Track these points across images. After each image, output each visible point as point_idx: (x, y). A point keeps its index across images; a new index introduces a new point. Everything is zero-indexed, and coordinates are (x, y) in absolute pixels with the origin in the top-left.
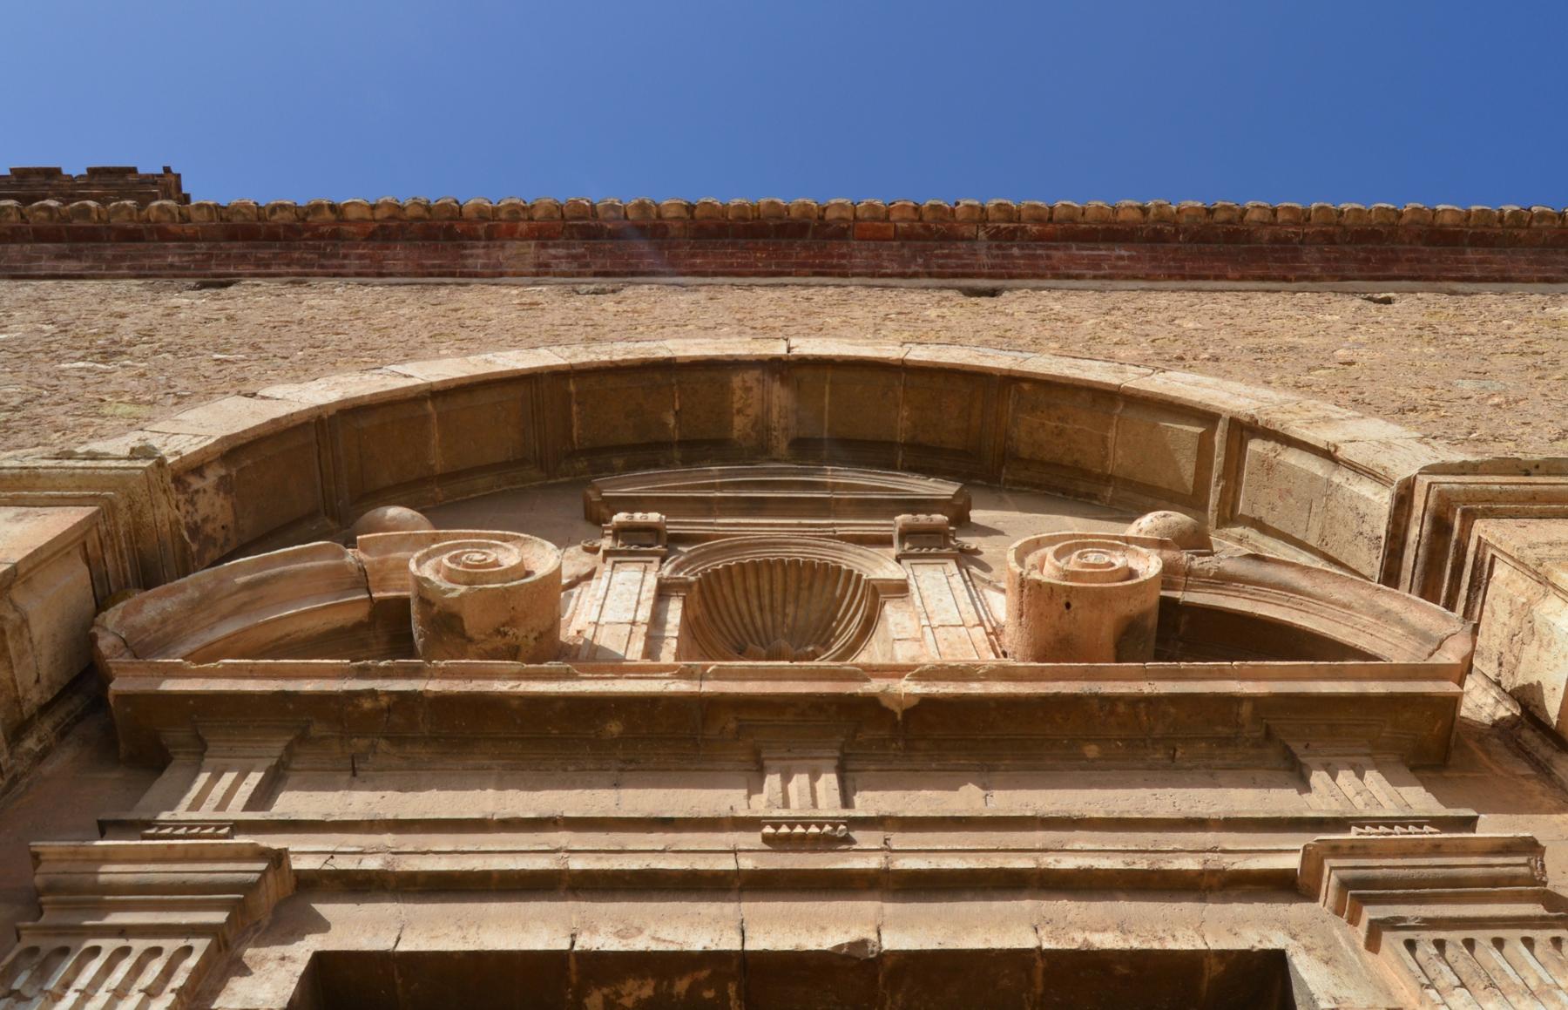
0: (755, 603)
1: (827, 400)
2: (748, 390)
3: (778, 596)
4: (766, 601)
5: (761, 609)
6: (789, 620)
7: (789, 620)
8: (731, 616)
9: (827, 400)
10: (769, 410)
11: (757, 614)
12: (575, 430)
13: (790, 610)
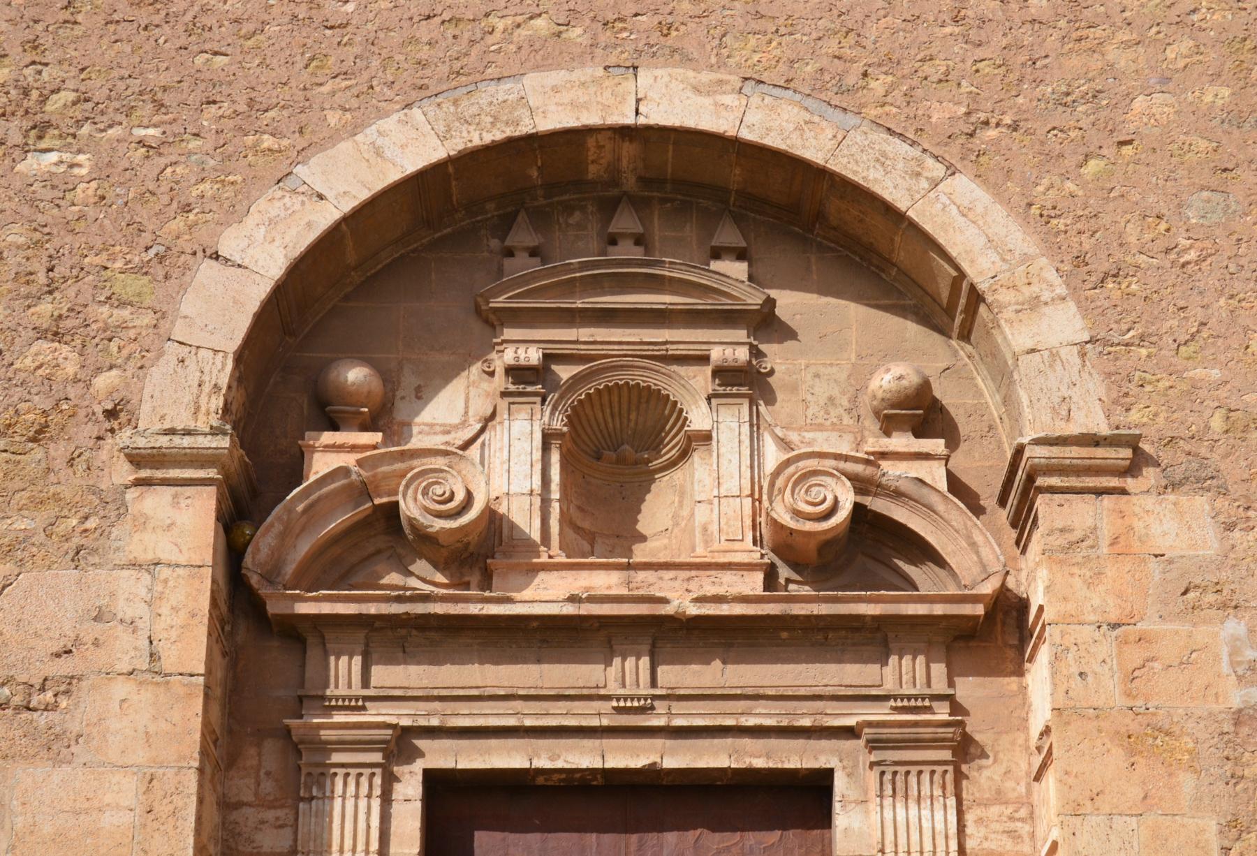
0: (608, 411)
1: (670, 154)
2: (600, 147)
3: (625, 407)
4: (616, 410)
5: (613, 416)
6: (632, 424)
7: (632, 424)
8: (591, 427)
9: (670, 154)
10: (619, 159)
11: (610, 420)
12: (454, 199)
13: (633, 416)
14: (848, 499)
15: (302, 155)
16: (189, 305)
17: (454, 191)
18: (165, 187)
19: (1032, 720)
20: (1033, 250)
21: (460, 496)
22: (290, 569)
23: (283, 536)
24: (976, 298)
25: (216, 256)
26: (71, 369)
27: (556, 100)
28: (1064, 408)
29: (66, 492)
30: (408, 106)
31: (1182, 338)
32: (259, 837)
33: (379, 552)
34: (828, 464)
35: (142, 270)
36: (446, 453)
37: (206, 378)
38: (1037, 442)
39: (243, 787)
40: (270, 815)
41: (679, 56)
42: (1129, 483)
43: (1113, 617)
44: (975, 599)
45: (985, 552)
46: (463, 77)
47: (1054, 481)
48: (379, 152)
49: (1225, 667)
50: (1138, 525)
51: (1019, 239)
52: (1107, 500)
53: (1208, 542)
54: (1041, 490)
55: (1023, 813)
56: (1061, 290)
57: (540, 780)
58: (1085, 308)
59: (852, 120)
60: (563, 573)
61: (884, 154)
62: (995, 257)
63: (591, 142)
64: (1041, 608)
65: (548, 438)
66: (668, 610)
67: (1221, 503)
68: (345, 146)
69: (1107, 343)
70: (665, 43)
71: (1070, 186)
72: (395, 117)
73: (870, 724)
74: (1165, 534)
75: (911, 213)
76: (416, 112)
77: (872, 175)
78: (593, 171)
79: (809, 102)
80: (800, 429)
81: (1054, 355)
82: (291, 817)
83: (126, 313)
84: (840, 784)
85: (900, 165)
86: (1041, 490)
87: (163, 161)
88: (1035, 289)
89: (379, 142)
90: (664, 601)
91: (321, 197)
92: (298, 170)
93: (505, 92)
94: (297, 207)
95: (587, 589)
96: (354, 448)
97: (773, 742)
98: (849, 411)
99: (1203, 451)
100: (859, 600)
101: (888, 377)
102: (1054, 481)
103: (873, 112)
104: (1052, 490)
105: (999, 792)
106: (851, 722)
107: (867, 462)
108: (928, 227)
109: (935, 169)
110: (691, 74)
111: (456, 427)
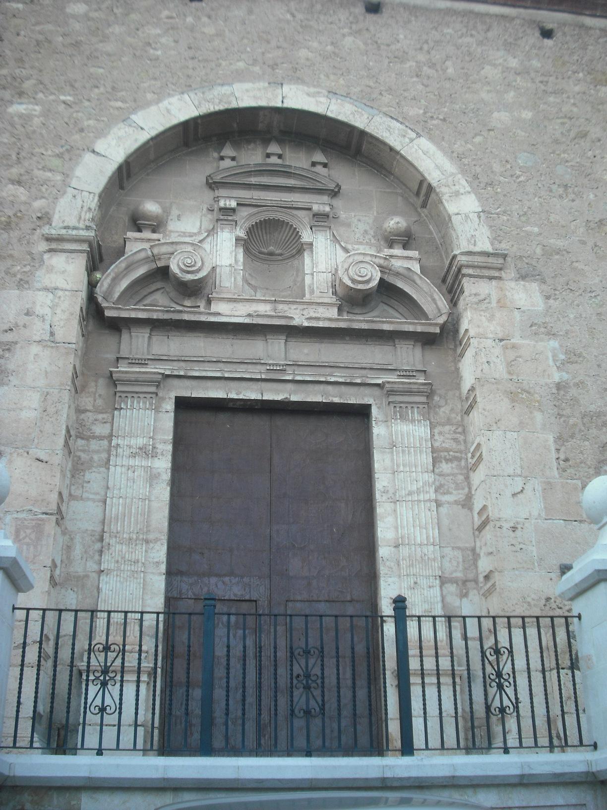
14: (377, 276)
15: (134, 110)
16: (79, 172)
17: (200, 131)
18: (72, 121)
19: (462, 384)
20: (455, 171)
21: (199, 264)
22: (116, 295)
23: (114, 279)
24: (430, 188)
25: (94, 151)
26: (23, 198)
27: (247, 95)
28: (473, 239)
29: (16, 253)
30: (183, 93)
31: (521, 213)
32: (93, 428)
33: (158, 290)
34: (368, 259)
35: (60, 156)
36: (193, 244)
37: (85, 204)
38: (462, 254)
39: (87, 401)
40: (100, 416)
41: (300, 80)
42: (503, 275)
43: (500, 336)
44: (436, 324)
45: (439, 303)
46: (208, 83)
47: (470, 271)
48: (168, 111)
49: (551, 362)
50: (508, 294)
51: (449, 166)
52: (494, 282)
53: (539, 304)
54: (464, 275)
55: (460, 430)
56: (468, 189)
57: (231, 405)
58: (479, 197)
59: (376, 112)
60: (245, 304)
61: (389, 126)
62: (439, 173)
63: (261, 113)
64: (467, 330)
65: (238, 239)
66: (295, 323)
67: (544, 287)
68: (153, 109)
69: (490, 213)
70: (296, 76)
71: (469, 146)
72: (176, 97)
73: (389, 382)
74: (521, 299)
75: (402, 152)
76: (186, 96)
77: (385, 134)
78: (261, 126)
79: (356, 103)
80: (352, 244)
81: (467, 217)
82: (110, 419)
83: (49, 174)
84: (374, 411)
85: (396, 132)
86: (464, 275)
87: (71, 110)
88: (457, 187)
89: (169, 107)
90: (292, 318)
91: (142, 128)
92: (133, 117)
93: (226, 90)
94: (131, 132)
95: (255, 312)
96: (149, 240)
97: (343, 389)
98: (374, 237)
99: (534, 263)
100: (383, 322)
101: (392, 222)
102: (470, 271)
103: (385, 109)
104: (470, 276)
105: (448, 419)
106: (380, 381)
107: (385, 259)
108: (409, 158)
109: (413, 135)
110: (306, 88)
111: (195, 234)
